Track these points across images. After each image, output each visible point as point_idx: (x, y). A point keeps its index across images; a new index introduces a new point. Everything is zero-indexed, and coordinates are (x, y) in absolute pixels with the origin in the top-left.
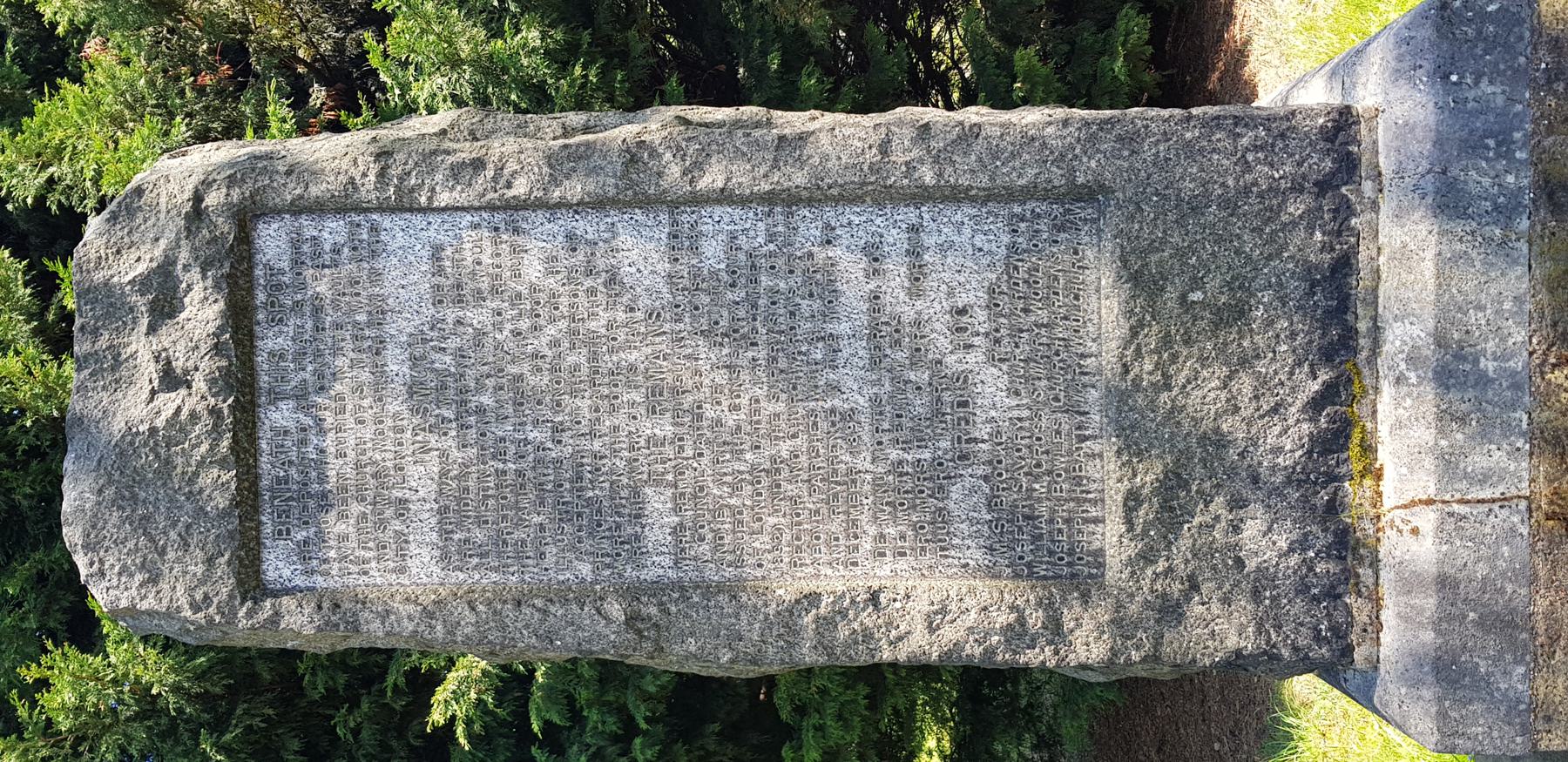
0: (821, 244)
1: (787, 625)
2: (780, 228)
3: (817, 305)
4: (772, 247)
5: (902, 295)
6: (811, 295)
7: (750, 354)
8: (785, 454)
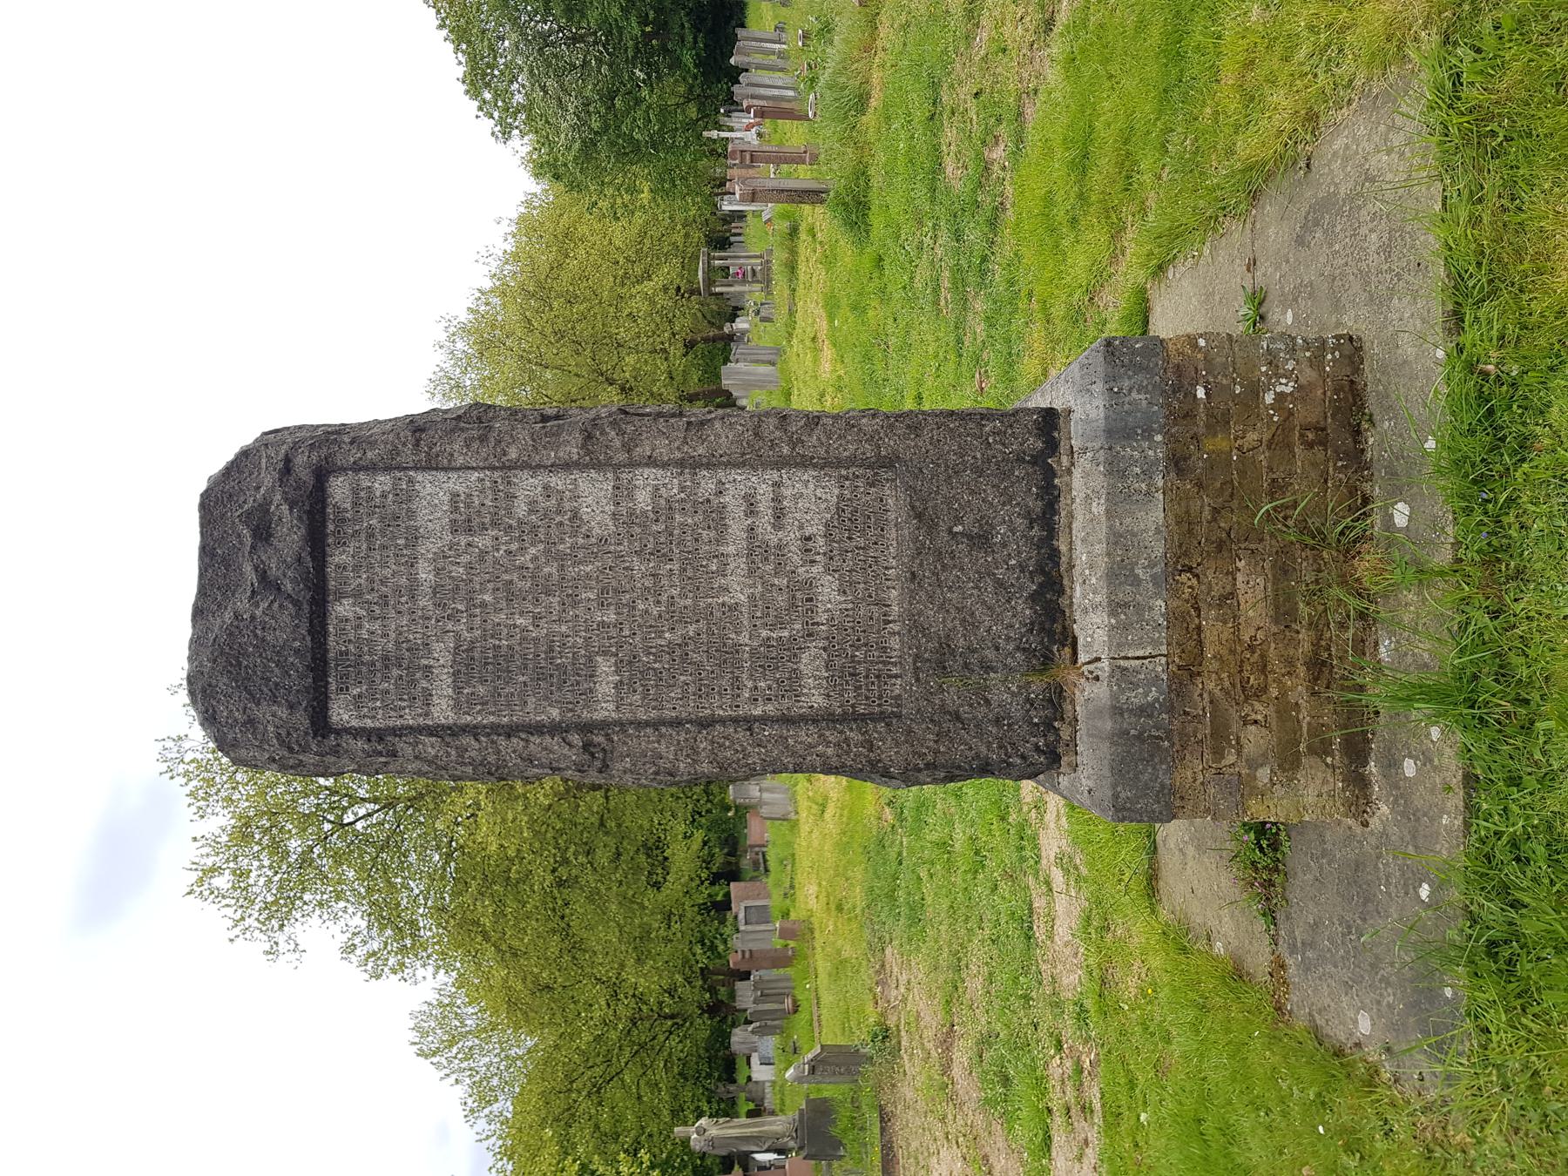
0: (715, 494)
1: (692, 748)
2: (688, 483)
3: (713, 534)
4: (683, 495)
5: (769, 528)
6: (709, 527)
7: (668, 567)
8: (691, 633)
